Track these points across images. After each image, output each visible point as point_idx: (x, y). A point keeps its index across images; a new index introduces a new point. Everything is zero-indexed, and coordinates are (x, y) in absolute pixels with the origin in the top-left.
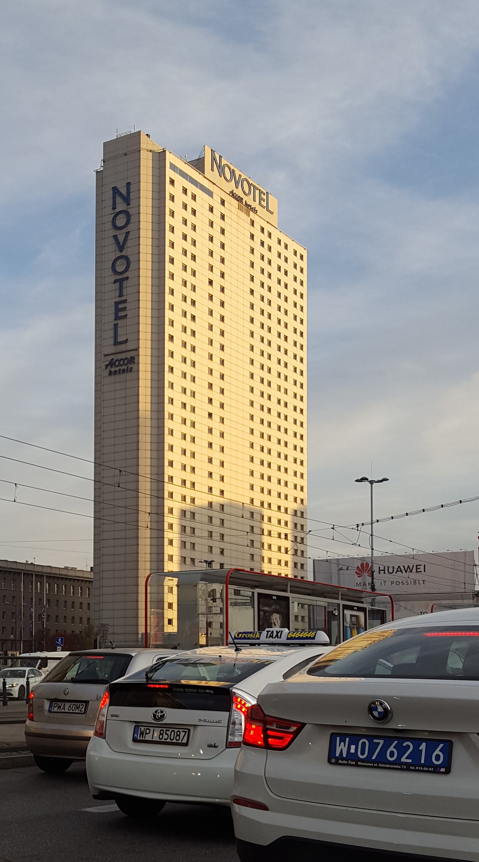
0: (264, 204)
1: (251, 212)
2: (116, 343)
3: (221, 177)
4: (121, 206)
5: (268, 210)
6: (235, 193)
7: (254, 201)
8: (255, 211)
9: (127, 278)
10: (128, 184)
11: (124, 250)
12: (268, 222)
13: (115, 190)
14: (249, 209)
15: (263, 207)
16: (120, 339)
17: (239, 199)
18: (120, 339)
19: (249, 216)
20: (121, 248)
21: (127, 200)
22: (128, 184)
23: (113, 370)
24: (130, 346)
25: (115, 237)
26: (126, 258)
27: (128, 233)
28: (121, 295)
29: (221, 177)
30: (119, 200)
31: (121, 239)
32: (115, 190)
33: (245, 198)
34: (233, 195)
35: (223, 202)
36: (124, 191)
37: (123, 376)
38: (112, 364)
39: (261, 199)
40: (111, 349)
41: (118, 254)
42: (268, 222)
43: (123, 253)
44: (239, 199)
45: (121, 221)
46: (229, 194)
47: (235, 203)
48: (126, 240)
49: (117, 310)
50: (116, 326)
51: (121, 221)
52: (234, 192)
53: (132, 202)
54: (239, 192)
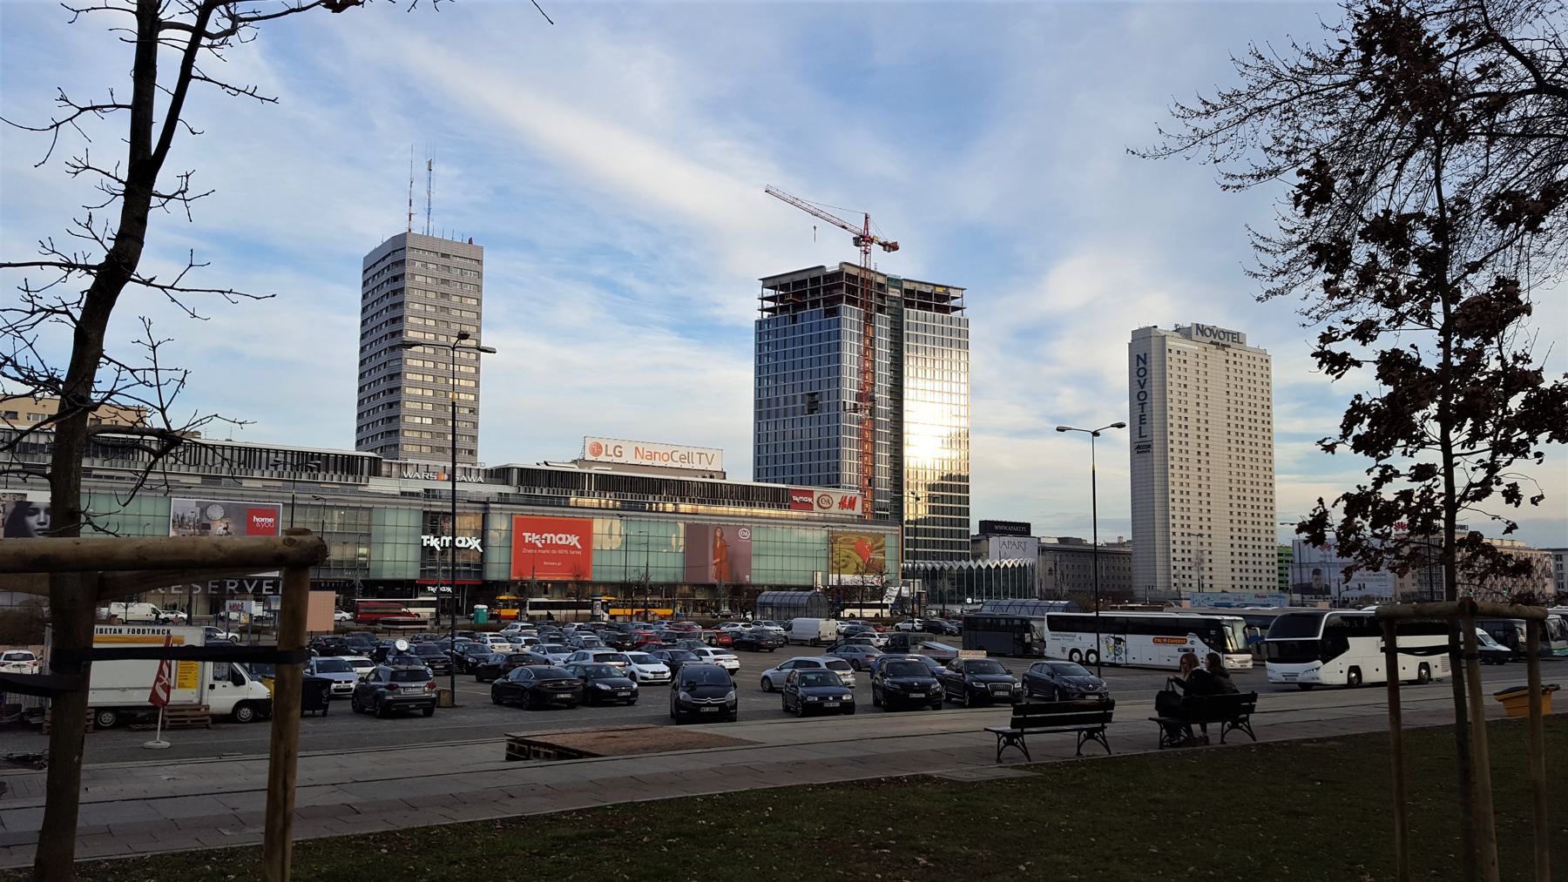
2: (1141, 437)
4: (1141, 365)
8: (1229, 346)
13: (1138, 356)
21: (1145, 362)
24: (1147, 439)
30: (1140, 361)
32: (1138, 356)
33: (1221, 342)
34: (1212, 343)
37: (1144, 455)
38: (1138, 447)
40: (1138, 440)
44: (1217, 344)
45: (1142, 373)
47: (1214, 347)
49: (1141, 420)
51: (1142, 373)
54: (1217, 340)
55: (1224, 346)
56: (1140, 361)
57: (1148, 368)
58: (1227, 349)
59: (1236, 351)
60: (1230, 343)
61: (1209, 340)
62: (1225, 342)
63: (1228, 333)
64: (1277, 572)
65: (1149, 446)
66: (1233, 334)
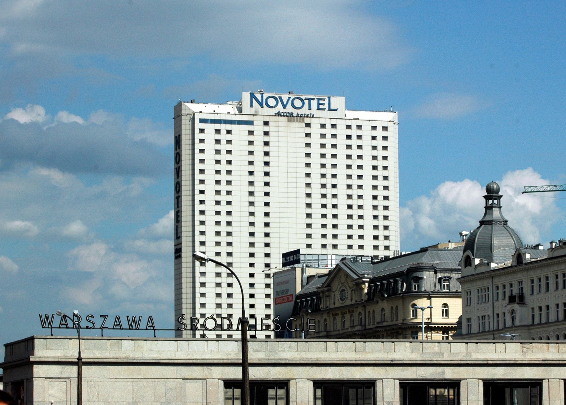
3: (262, 107)
5: (330, 109)
6: (282, 113)
7: (310, 109)
12: (330, 119)
15: (324, 109)
16: (178, 236)
17: (290, 116)
18: (178, 236)
19: (303, 121)
23: (177, 255)
25: (176, 168)
29: (262, 107)
33: (295, 112)
34: (278, 114)
35: (266, 123)
39: (319, 104)
44: (290, 116)
46: (275, 116)
50: (177, 226)
52: (281, 112)
54: (289, 109)
55: (301, 117)
58: (307, 120)
61: (275, 111)
62: (305, 111)
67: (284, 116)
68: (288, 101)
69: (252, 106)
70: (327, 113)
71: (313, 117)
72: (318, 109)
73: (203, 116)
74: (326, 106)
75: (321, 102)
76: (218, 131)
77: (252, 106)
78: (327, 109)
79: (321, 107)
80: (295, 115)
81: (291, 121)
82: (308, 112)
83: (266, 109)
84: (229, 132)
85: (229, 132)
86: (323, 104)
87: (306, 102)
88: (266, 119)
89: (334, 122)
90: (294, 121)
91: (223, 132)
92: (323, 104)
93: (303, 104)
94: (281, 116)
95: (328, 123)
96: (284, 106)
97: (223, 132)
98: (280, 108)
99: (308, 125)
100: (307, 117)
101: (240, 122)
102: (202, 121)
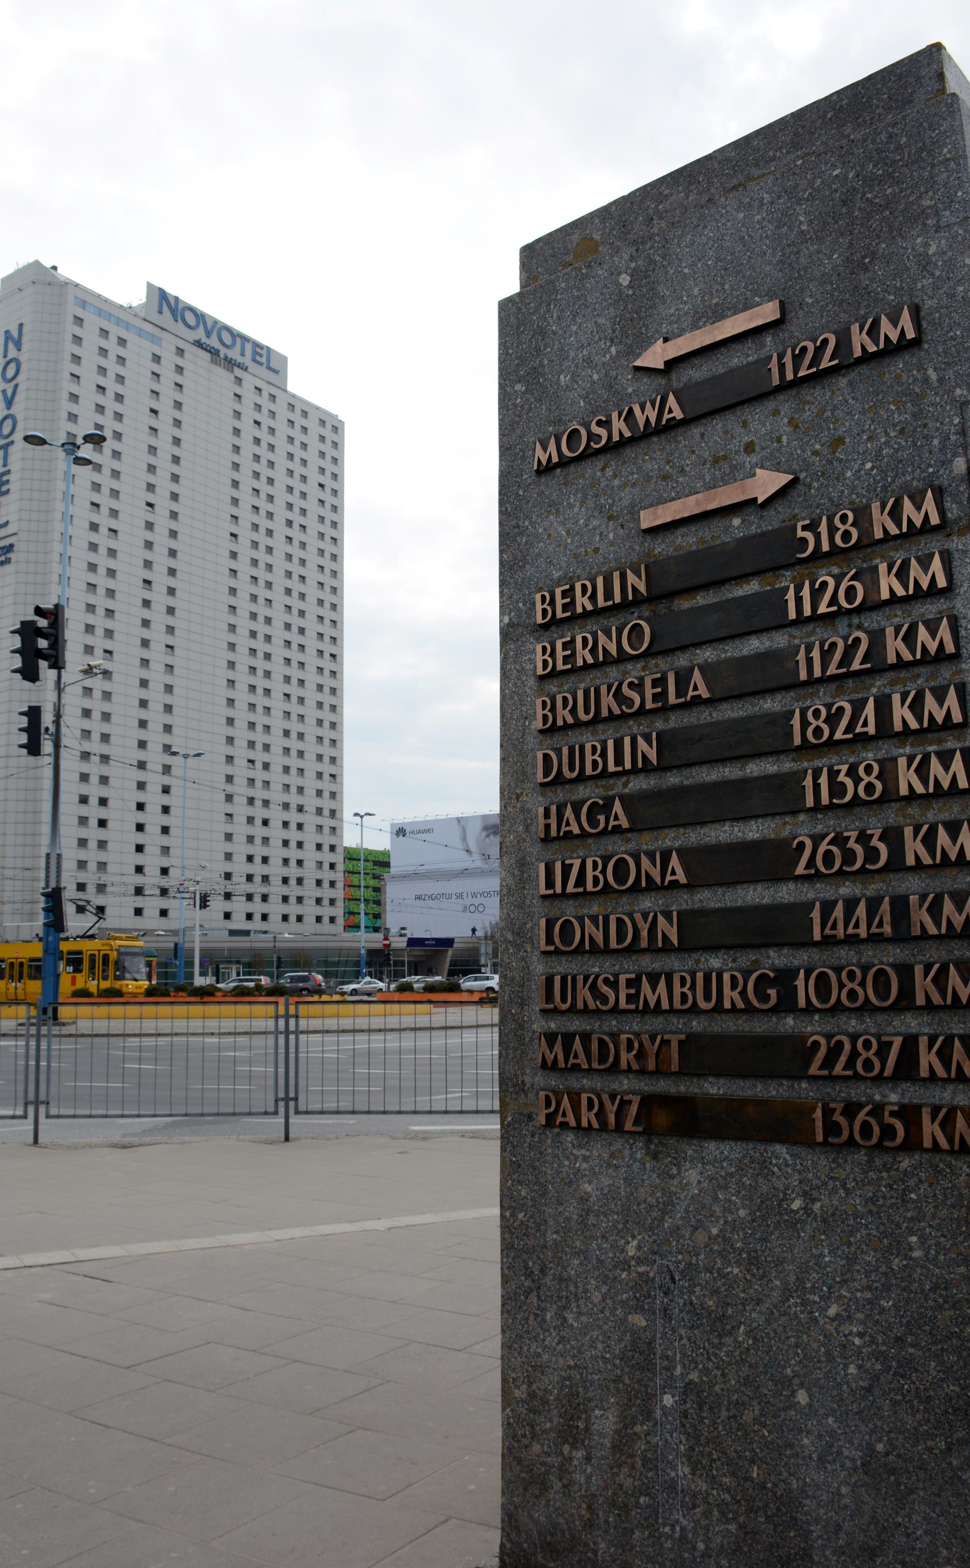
0: (263, 360)
1: (236, 369)
3: (176, 321)
4: (12, 353)
5: (269, 368)
7: (243, 355)
9: (12, 442)
10: (21, 325)
11: (13, 407)
12: (269, 383)
14: (230, 364)
15: (261, 364)
17: (214, 353)
19: (232, 372)
20: (9, 403)
21: (18, 345)
22: (21, 325)
25: (4, 392)
26: (13, 417)
27: (16, 386)
28: (5, 465)
29: (176, 321)
30: (11, 346)
31: (9, 393)
33: (223, 351)
34: (198, 344)
35: (180, 352)
36: (15, 334)
39: (255, 353)
41: (6, 412)
42: (269, 383)
43: (11, 412)
44: (214, 353)
47: (207, 356)
48: (14, 393)
53: (25, 347)
54: (214, 342)
55: (230, 364)
56: (11, 346)
57: (23, 357)
58: (238, 372)
59: (260, 384)
60: (247, 360)
62: (234, 354)
63: (245, 339)
64: (340, 867)
65: (12, 546)
66: (256, 345)
67: (206, 349)
68: (213, 327)
69: (160, 312)
70: (262, 371)
71: (246, 369)
72: (254, 360)
73: (82, 296)
74: (263, 360)
75: (258, 350)
76: (104, 333)
77: (160, 312)
78: (265, 365)
79: (258, 358)
80: (222, 356)
81: (216, 364)
82: (239, 359)
83: (180, 328)
84: (122, 342)
85: (122, 342)
86: (261, 356)
87: (238, 340)
88: (182, 345)
89: (274, 391)
90: (220, 365)
91: (113, 338)
92: (261, 356)
93: (234, 342)
94: (203, 348)
95: (267, 389)
96: (208, 334)
97: (113, 338)
98: (200, 334)
99: (239, 381)
100: (239, 366)
101: (141, 333)
102: (83, 304)
